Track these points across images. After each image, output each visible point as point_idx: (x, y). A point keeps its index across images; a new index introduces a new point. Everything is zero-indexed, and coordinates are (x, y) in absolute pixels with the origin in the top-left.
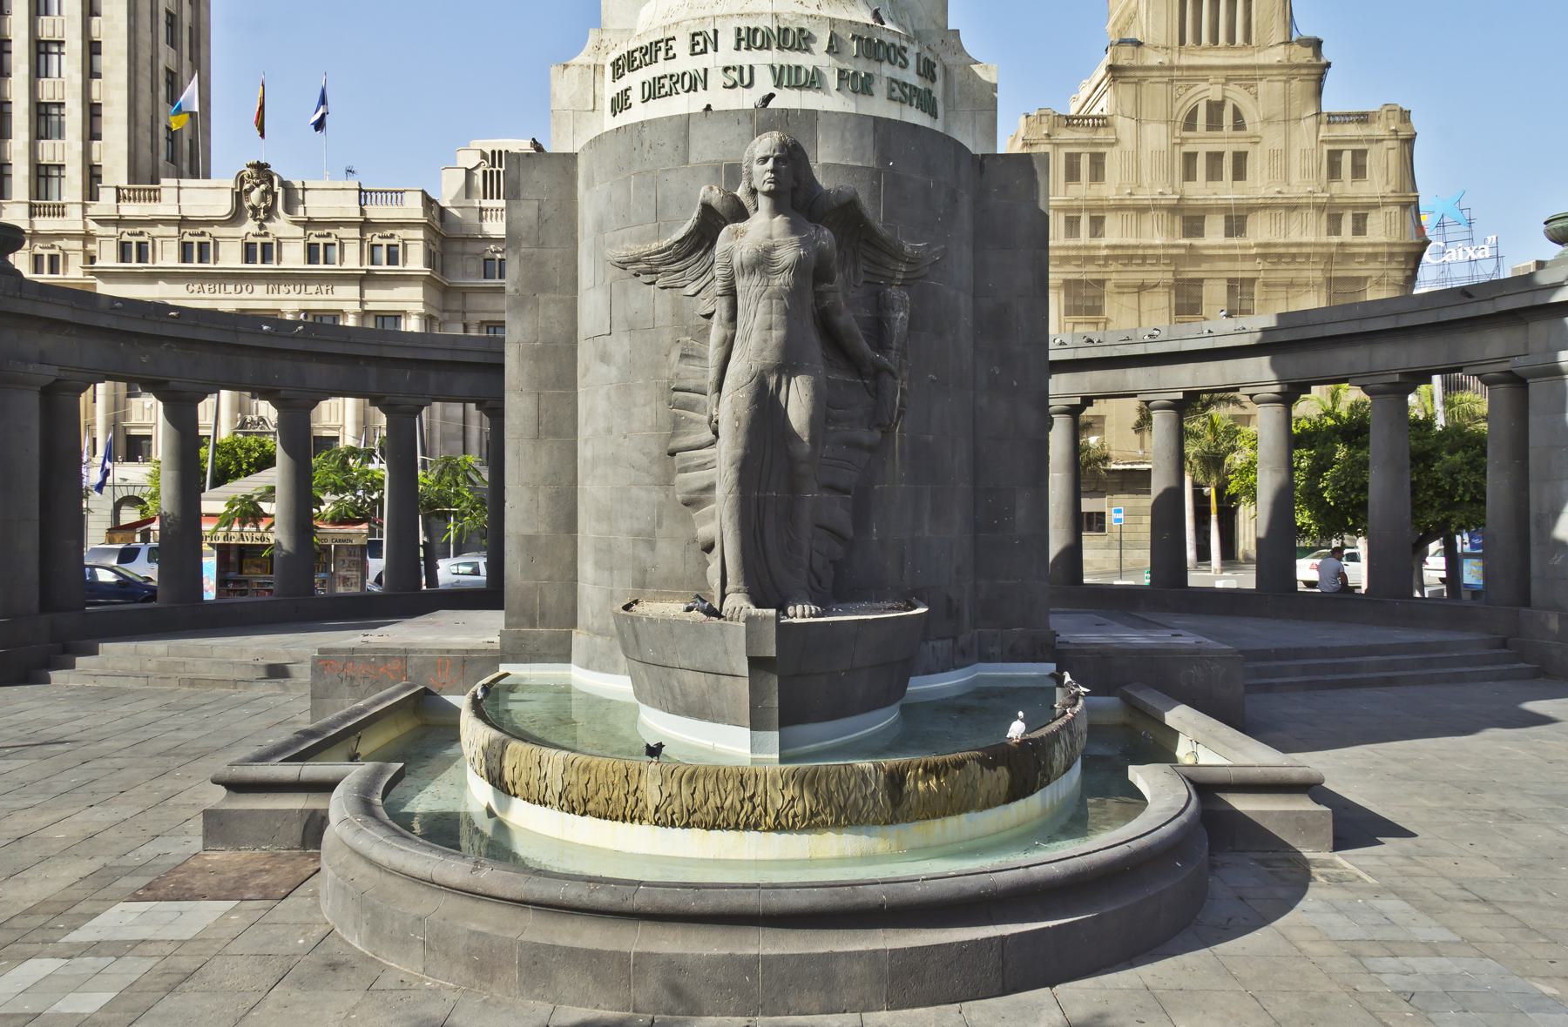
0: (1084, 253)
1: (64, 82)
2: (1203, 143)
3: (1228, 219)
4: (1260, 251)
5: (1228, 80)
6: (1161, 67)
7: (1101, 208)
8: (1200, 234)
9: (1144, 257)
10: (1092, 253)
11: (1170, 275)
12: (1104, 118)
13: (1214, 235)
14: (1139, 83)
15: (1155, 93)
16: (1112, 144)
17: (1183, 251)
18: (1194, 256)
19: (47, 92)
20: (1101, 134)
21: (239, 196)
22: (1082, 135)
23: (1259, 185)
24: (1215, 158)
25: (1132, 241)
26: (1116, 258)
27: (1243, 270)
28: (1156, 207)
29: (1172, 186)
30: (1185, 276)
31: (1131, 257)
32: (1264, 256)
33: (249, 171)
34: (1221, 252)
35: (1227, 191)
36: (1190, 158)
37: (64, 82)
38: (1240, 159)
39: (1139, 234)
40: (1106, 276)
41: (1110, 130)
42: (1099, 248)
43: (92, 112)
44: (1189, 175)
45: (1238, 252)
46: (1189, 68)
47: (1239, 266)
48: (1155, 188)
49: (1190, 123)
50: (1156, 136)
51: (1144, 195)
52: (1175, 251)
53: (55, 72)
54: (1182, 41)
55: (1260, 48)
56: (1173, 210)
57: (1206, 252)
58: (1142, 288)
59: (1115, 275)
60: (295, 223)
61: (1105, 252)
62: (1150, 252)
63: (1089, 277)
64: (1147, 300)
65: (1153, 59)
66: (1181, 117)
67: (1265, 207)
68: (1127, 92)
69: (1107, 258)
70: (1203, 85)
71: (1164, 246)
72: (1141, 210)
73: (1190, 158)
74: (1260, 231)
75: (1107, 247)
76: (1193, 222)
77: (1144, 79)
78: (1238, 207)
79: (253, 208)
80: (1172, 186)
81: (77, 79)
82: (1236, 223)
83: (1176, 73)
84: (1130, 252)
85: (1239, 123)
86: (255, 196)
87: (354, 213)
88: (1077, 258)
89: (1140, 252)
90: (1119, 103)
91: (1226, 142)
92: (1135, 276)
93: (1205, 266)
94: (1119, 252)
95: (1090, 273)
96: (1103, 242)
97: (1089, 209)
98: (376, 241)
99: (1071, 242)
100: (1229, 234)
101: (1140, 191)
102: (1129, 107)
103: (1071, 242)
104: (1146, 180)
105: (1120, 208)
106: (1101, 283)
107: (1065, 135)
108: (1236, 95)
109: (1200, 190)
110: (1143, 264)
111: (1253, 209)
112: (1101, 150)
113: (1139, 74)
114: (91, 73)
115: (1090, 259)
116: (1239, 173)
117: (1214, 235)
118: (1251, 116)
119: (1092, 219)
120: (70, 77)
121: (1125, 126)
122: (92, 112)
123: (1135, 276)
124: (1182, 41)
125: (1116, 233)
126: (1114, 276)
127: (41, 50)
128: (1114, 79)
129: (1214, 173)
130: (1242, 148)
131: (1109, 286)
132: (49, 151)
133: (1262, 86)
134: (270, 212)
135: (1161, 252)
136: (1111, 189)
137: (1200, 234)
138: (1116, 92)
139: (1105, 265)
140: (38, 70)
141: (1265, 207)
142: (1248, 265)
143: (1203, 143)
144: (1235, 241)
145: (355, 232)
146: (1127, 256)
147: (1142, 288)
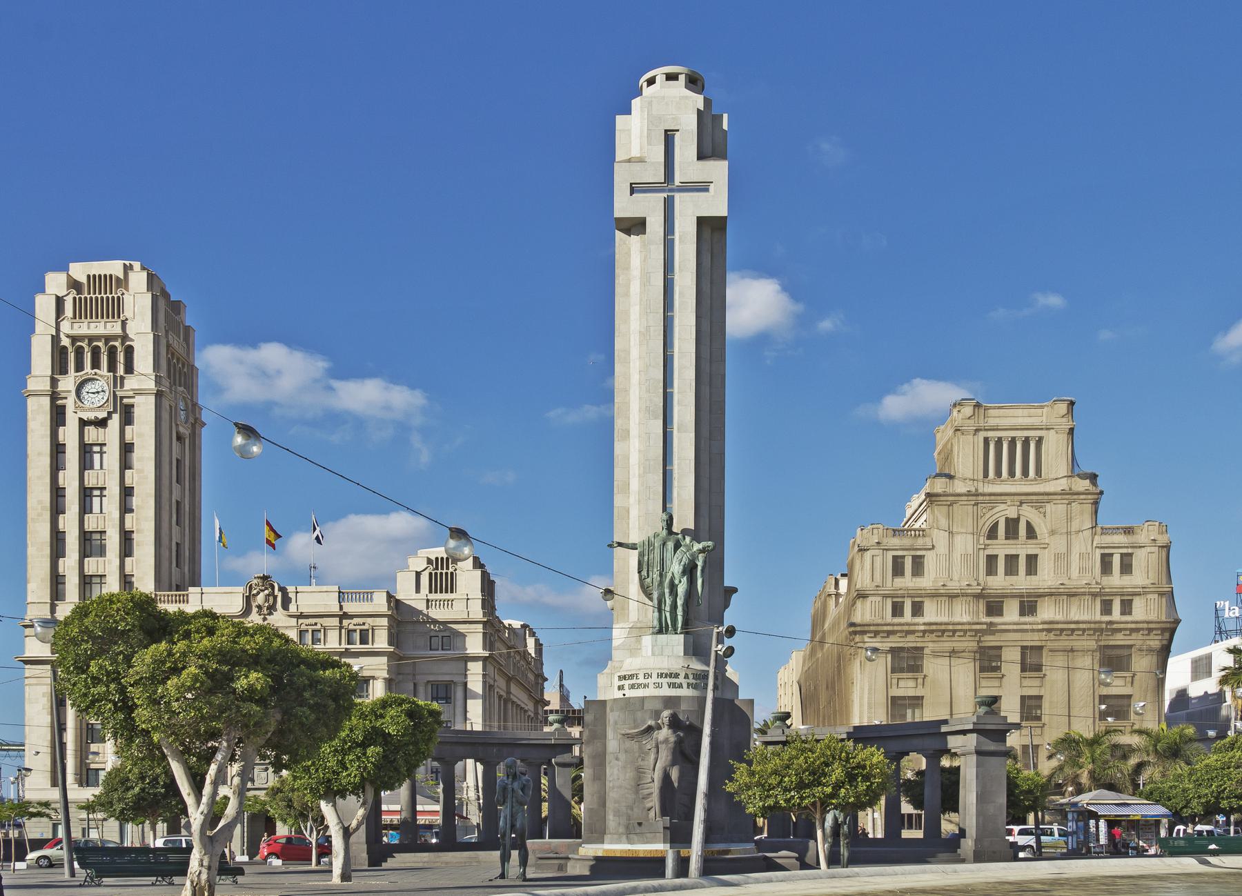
1: (106, 516)
3: (1022, 603)
4: (1046, 626)
8: (1001, 614)
13: (1011, 614)
19: (91, 523)
20: (920, 542)
21: (248, 600)
22: (906, 542)
23: (1046, 577)
24: (1012, 560)
33: (255, 581)
35: (1022, 582)
36: (992, 560)
37: (106, 516)
39: (951, 613)
43: (127, 539)
48: (961, 579)
50: (964, 543)
51: (954, 586)
53: (96, 508)
56: (978, 596)
60: (290, 616)
67: (1051, 594)
68: (940, 512)
72: (952, 597)
73: (992, 560)
74: (1047, 612)
76: (994, 608)
79: (259, 607)
81: (117, 514)
82: (1028, 606)
86: (260, 599)
87: (335, 609)
98: (351, 627)
100: (1022, 614)
105: (934, 595)
107: (896, 542)
109: (999, 582)
112: (919, 553)
114: (125, 509)
117: (1011, 614)
120: (110, 513)
122: (127, 539)
125: (933, 613)
127: (86, 494)
129: (1011, 569)
132: (92, 565)
134: (272, 609)
136: (927, 582)
137: (1001, 614)
140: (85, 508)
141: (1051, 594)
145: (335, 621)
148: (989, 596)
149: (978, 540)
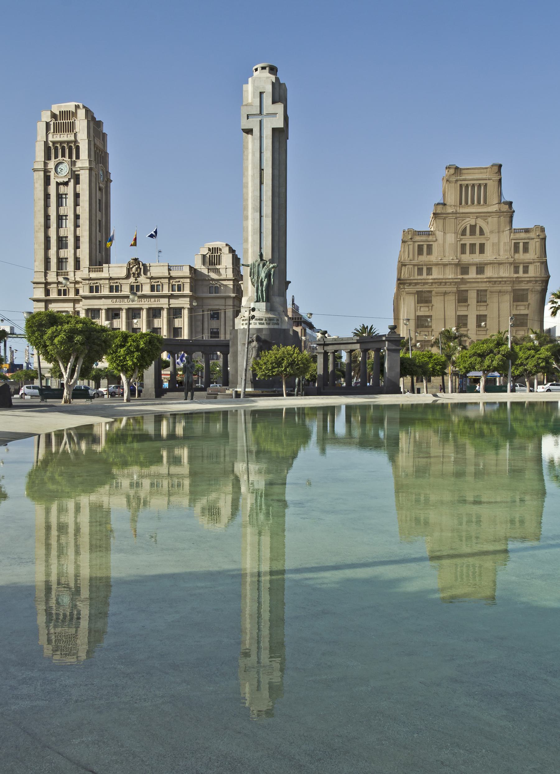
0: (423, 281)
2: (468, 240)
4: (488, 280)
5: (477, 217)
6: (453, 213)
7: (430, 265)
9: (446, 283)
10: (427, 281)
11: (455, 289)
12: (432, 232)
13: (473, 274)
14: (445, 219)
15: (450, 222)
16: (434, 241)
17: (459, 280)
18: (463, 281)
20: (431, 238)
22: (424, 238)
24: (473, 246)
25: (441, 277)
26: (435, 283)
27: (483, 286)
28: (450, 264)
29: (456, 256)
30: (463, 289)
31: (441, 283)
32: (490, 282)
34: (474, 280)
35: (477, 258)
36: (463, 246)
38: (482, 246)
39: (444, 274)
40: (432, 289)
41: (434, 236)
42: (428, 279)
44: (463, 252)
45: (479, 280)
46: (463, 213)
47: (480, 285)
48: (450, 257)
49: (464, 233)
50: (451, 238)
51: (445, 260)
52: (456, 280)
54: (461, 204)
55: (489, 206)
56: (457, 265)
57: (468, 280)
58: (445, 294)
59: (435, 289)
61: (431, 281)
62: (447, 281)
63: (425, 289)
64: (447, 298)
65: (450, 210)
66: (460, 232)
67: (490, 264)
68: (440, 222)
69: (432, 283)
70: (468, 219)
71: (452, 279)
72: (445, 265)
75: (432, 279)
76: (465, 269)
77: (446, 217)
78: (480, 264)
80: (456, 256)
82: (480, 269)
83: (458, 215)
84: (440, 281)
85: (482, 232)
88: (421, 283)
89: (444, 281)
90: (437, 227)
91: (477, 240)
92: (443, 289)
93: (468, 285)
94: (436, 281)
95: (426, 288)
96: (430, 277)
97: (426, 265)
99: (419, 277)
101: (444, 258)
102: (441, 227)
103: (419, 277)
104: (447, 254)
105: (437, 265)
106: (430, 292)
108: (481, 223)
109: (467, 258)
110: (445, 285)
111: (487, 264)
112: (431, 243)
113: (444, 215)
115: (425, 284)
116: (482, 251)
117: (473, 274)
118: (486, 230)
119: (427, 268)
121: (439, 235)
123: (443, 289)
124: (461, 204)
125: (436, 274)
126: (435, 289)
128: (435, 218)
130: (483, 242)
131: (433, 292)
133: (490, 219)
135: (451, 280)
136: (433, 258)
138: (436, 222)
139: (432, 285)
141: (490, 264)
142: (484, 285)
143: (468, 240)
144: (479, 276)
146: (439, 282)
147: (445, 294)
148: (463, 264)
149: (457, 236)
